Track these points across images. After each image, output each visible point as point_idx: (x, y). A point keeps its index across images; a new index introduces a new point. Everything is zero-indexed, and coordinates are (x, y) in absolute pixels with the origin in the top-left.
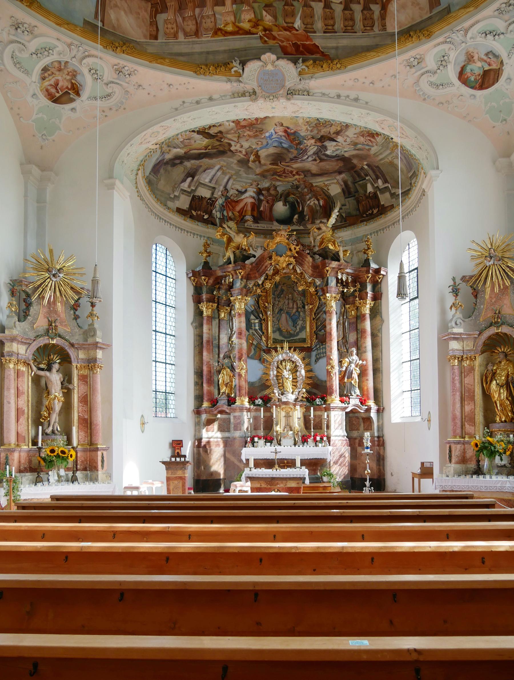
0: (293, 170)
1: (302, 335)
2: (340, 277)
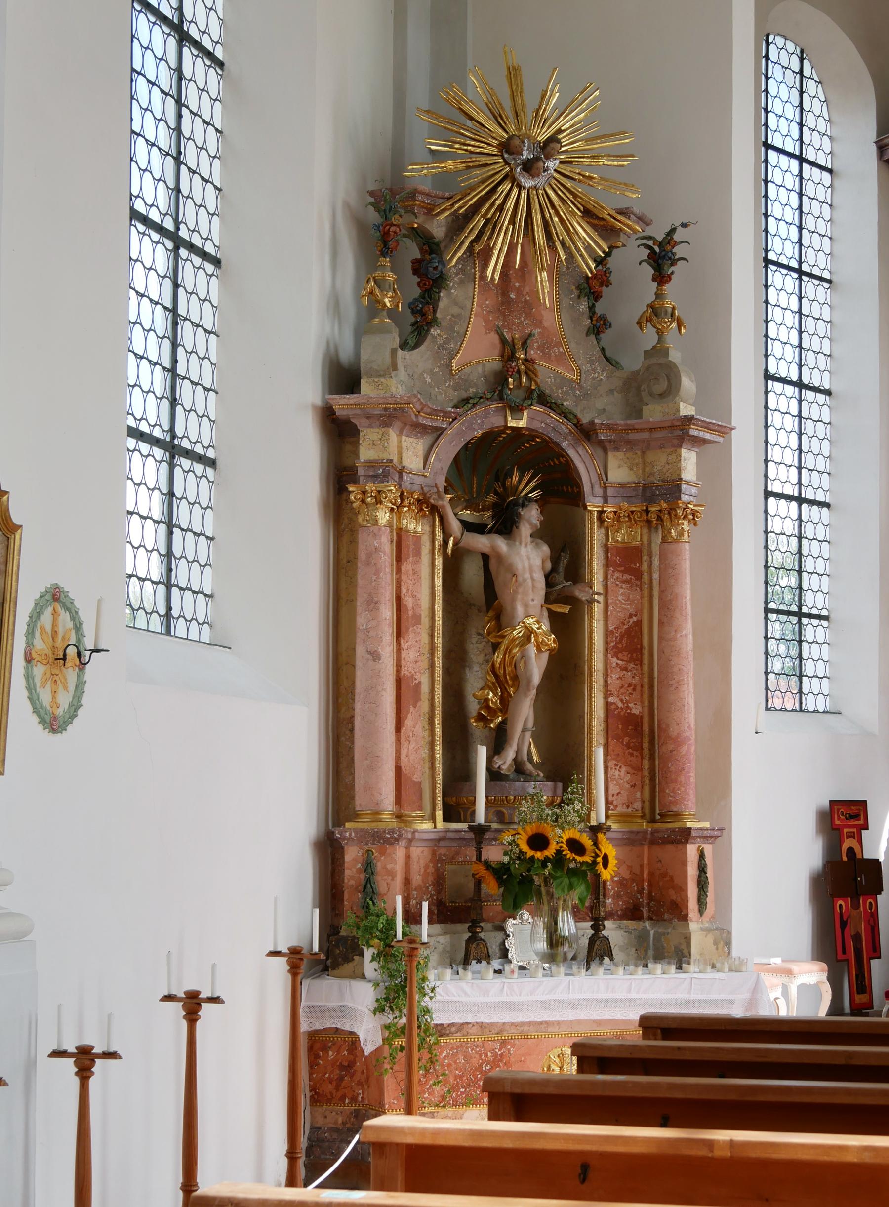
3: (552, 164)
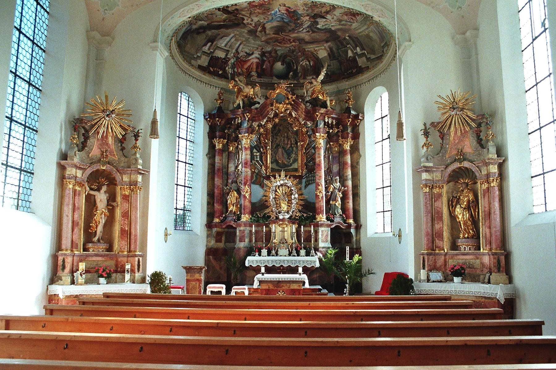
0: (290, 38)
1: (295, 166)
2: (326, 121)
3: (114, 116)
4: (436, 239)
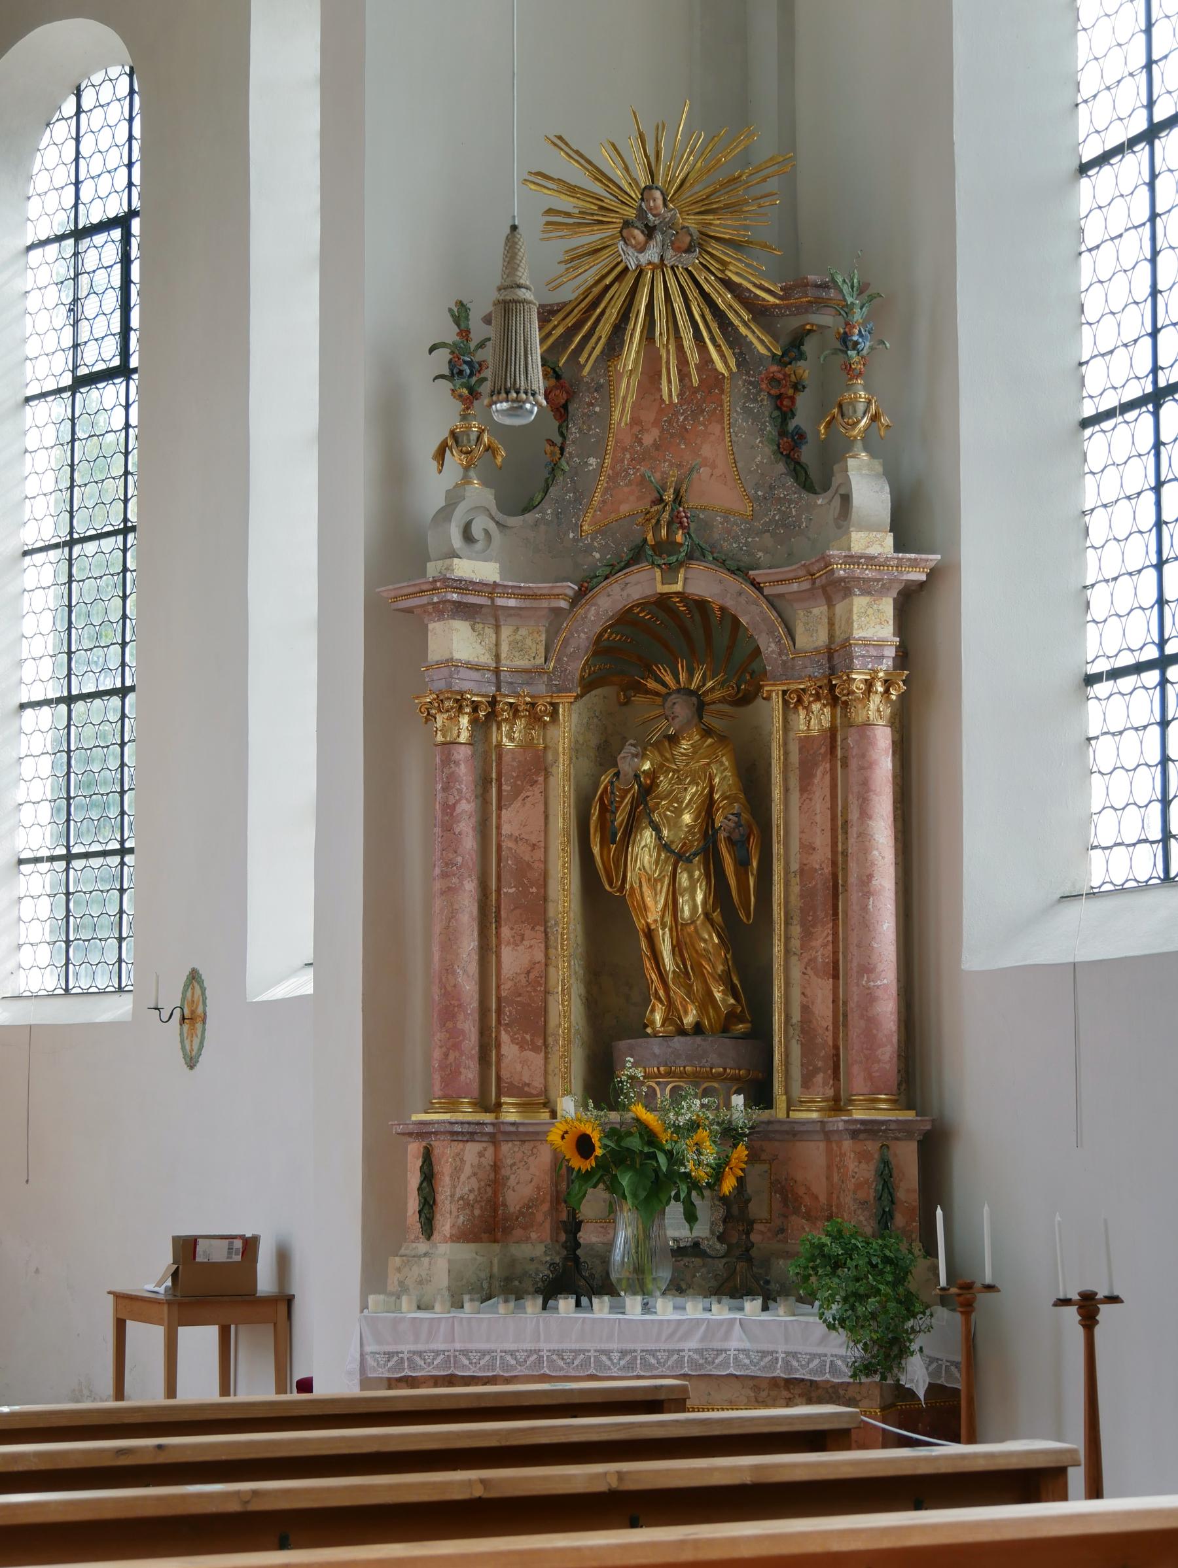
4: (505, 1037)
